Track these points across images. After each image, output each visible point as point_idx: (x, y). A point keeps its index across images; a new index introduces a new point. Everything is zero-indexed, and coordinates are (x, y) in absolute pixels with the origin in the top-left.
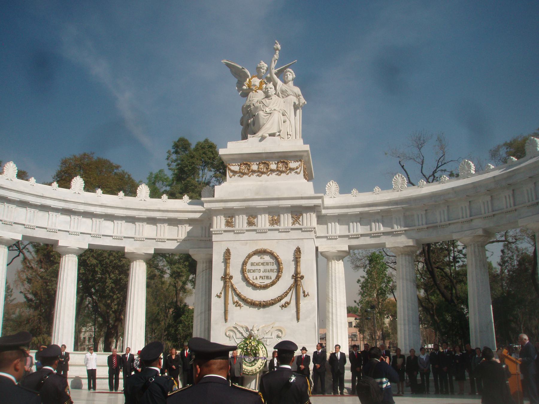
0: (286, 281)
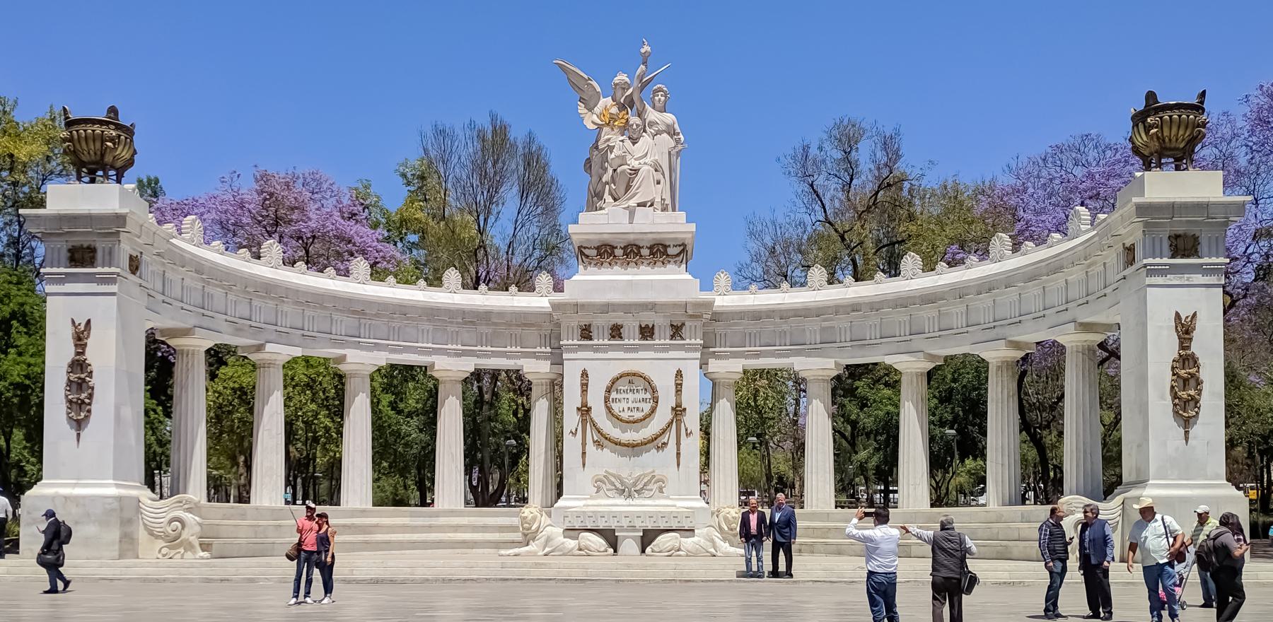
0: (664, 415)
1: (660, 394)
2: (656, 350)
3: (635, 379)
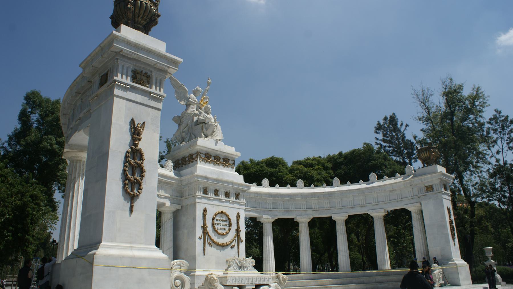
0: (233, 233)
1: (232, 222)
2: (230, 203)
3: (223, 215)
